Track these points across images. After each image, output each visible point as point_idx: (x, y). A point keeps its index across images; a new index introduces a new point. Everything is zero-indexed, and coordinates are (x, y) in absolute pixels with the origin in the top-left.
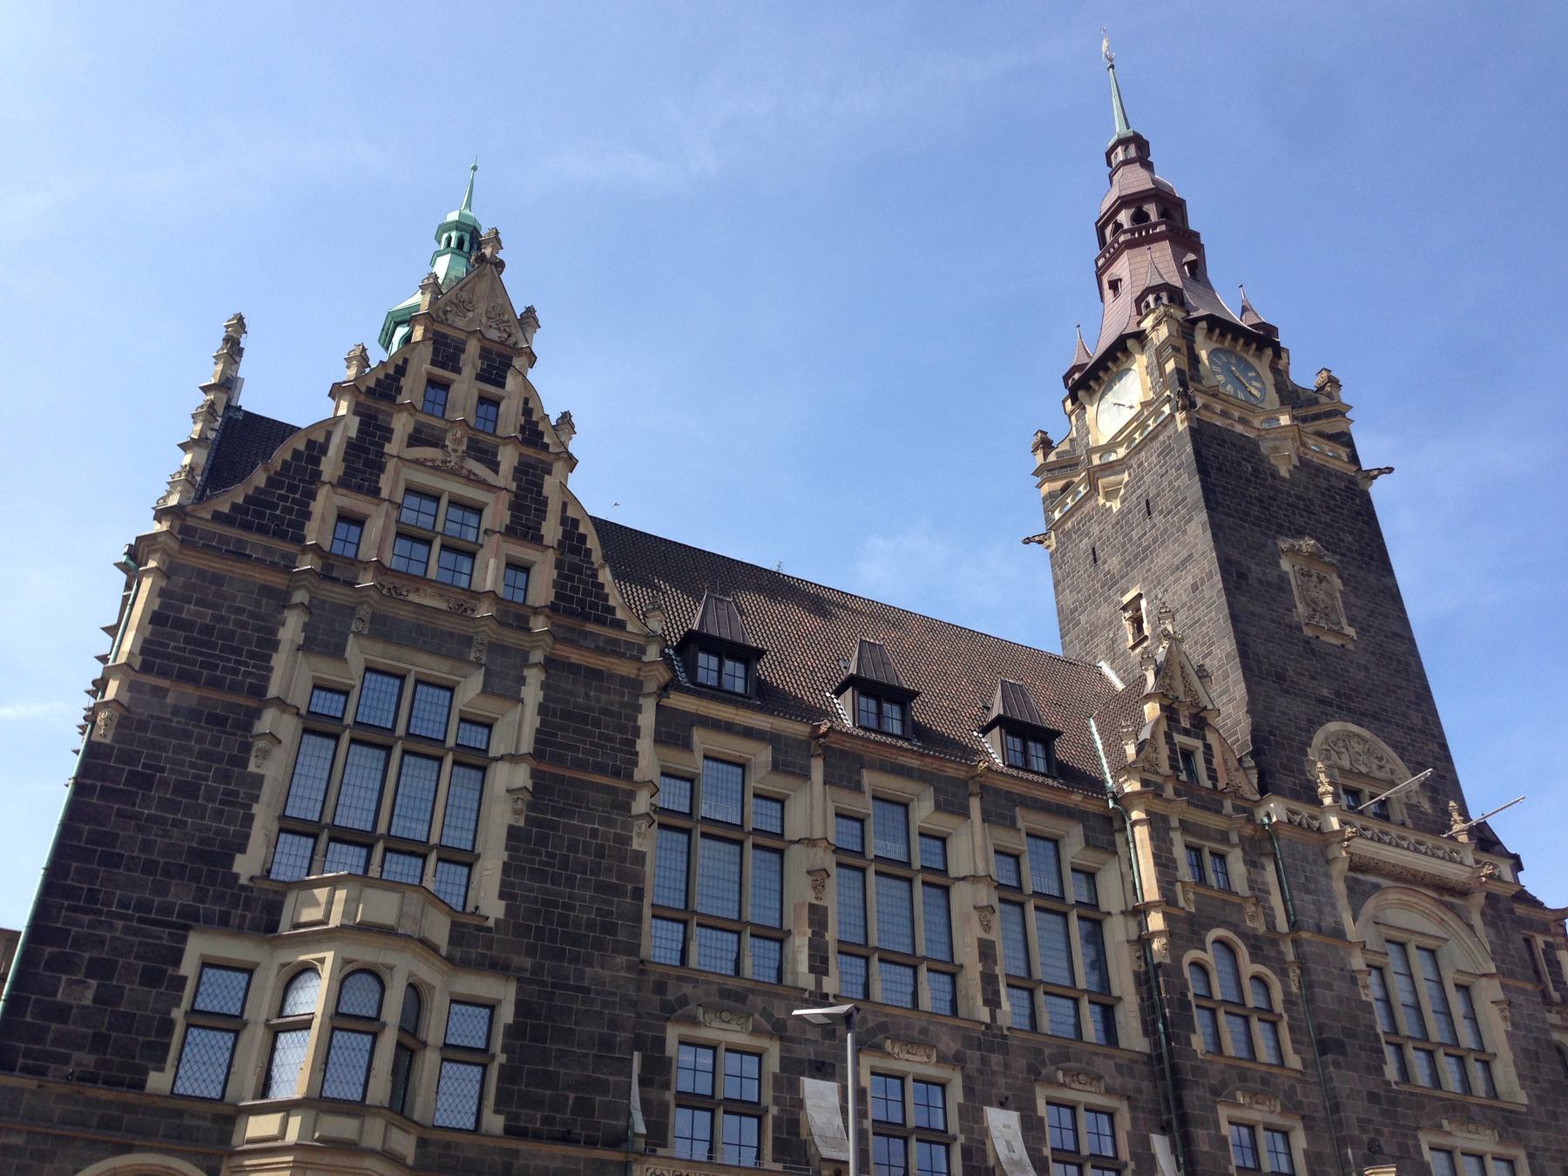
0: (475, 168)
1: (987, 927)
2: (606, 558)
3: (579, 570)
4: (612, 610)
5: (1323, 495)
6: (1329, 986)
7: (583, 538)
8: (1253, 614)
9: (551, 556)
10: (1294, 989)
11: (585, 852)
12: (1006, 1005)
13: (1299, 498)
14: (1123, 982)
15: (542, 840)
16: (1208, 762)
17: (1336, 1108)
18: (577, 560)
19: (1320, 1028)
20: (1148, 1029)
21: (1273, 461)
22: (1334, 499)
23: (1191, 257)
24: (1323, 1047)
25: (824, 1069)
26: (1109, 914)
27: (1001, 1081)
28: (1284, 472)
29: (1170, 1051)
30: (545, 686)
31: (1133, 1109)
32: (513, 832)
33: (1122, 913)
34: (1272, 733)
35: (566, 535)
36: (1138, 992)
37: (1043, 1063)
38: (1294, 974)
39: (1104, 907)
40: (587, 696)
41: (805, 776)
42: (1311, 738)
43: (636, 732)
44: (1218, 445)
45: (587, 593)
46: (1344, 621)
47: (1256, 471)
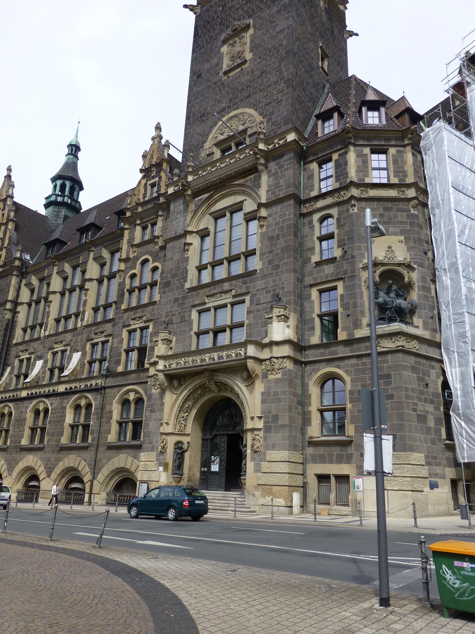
0: (79, 123)
6: (172, 259)
12: (86, 319)
25: (40, 358)
27: (79, 344)
37: (91, 333)
42: (208, 138)
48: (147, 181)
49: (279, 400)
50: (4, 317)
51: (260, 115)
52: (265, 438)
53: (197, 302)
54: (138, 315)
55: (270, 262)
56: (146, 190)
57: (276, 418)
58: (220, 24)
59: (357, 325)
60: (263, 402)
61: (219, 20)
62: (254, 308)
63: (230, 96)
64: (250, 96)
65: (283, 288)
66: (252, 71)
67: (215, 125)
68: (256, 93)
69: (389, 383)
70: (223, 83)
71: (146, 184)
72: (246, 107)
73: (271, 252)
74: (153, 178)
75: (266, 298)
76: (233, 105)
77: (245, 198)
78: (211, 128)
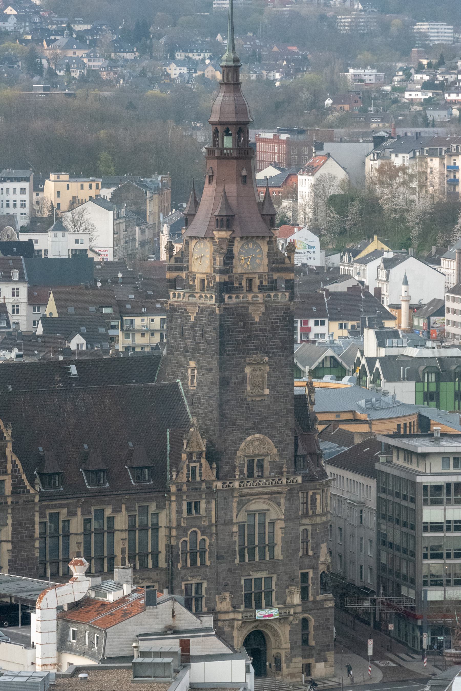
1: (124, 544)
2: (24, 472)
3: (16, 477)
4: (26, 487)
5: (272, 323)
6: (223, 539)
7: (17, 465)
8: (228, 400)
9: (10, 476)
10: (213, 540)
11: (25, 561)
13: (261, 330)
14: (162, 548)
15: (16, 561)
16: (200, 470)
17: (217, 575)
18: (16, 474)
19: (218, 553)
20: (167, 561)
21: (253, 315)
22: (276, 323)
23: (244, 173)
24: (217, 558)
26: (161, 527)
28: (257, 319)
29: (172, 569)
30: (13, 518)
31: (159, 584)
32: (10, 561)
33: (165, 527)
34: (225, 450)
35: (13, 467)
36: (166, 550)
38: (214, 536)
39: (160, 525)
40: (22, 517)
41: (76, 514)
42: (239, 447)
43: (34, 523)
44: (231, 318)
45: (20, 484)
46: (265, 386)
47: (244, 324)
48: (189, 462)
49: (297, 634)
50: (34, 554)
51: (276, 447)
52: (291, 652)
53: (244, 574)
54: (193, 574)
55: (287, 557)
56: (188, 471)
57: (296, 642)
58: (243, 340)
59: (318, 595)
60: (290, 635)
61: (241, 337)
62: (278, 583)
63: (255, 420)
64: (268, 428)
65: (294, 573)
66: (269, 405)
67: (245, 439)
68: (272, 428)
69: (328, 622)
70: (248, 404)
71: (188, 465)
72: (266, 435)
73: (288, 550)
74: (195, 462)
75: (285, 578)
76: (256, 429)
77: (269, 508)
78: (242, 440)
